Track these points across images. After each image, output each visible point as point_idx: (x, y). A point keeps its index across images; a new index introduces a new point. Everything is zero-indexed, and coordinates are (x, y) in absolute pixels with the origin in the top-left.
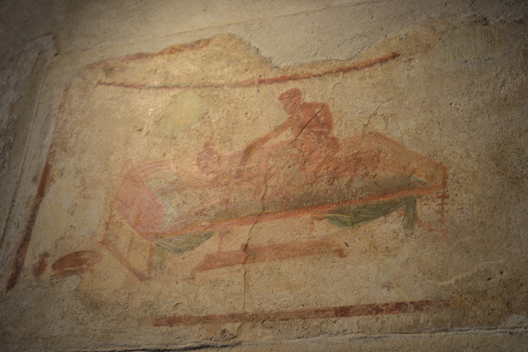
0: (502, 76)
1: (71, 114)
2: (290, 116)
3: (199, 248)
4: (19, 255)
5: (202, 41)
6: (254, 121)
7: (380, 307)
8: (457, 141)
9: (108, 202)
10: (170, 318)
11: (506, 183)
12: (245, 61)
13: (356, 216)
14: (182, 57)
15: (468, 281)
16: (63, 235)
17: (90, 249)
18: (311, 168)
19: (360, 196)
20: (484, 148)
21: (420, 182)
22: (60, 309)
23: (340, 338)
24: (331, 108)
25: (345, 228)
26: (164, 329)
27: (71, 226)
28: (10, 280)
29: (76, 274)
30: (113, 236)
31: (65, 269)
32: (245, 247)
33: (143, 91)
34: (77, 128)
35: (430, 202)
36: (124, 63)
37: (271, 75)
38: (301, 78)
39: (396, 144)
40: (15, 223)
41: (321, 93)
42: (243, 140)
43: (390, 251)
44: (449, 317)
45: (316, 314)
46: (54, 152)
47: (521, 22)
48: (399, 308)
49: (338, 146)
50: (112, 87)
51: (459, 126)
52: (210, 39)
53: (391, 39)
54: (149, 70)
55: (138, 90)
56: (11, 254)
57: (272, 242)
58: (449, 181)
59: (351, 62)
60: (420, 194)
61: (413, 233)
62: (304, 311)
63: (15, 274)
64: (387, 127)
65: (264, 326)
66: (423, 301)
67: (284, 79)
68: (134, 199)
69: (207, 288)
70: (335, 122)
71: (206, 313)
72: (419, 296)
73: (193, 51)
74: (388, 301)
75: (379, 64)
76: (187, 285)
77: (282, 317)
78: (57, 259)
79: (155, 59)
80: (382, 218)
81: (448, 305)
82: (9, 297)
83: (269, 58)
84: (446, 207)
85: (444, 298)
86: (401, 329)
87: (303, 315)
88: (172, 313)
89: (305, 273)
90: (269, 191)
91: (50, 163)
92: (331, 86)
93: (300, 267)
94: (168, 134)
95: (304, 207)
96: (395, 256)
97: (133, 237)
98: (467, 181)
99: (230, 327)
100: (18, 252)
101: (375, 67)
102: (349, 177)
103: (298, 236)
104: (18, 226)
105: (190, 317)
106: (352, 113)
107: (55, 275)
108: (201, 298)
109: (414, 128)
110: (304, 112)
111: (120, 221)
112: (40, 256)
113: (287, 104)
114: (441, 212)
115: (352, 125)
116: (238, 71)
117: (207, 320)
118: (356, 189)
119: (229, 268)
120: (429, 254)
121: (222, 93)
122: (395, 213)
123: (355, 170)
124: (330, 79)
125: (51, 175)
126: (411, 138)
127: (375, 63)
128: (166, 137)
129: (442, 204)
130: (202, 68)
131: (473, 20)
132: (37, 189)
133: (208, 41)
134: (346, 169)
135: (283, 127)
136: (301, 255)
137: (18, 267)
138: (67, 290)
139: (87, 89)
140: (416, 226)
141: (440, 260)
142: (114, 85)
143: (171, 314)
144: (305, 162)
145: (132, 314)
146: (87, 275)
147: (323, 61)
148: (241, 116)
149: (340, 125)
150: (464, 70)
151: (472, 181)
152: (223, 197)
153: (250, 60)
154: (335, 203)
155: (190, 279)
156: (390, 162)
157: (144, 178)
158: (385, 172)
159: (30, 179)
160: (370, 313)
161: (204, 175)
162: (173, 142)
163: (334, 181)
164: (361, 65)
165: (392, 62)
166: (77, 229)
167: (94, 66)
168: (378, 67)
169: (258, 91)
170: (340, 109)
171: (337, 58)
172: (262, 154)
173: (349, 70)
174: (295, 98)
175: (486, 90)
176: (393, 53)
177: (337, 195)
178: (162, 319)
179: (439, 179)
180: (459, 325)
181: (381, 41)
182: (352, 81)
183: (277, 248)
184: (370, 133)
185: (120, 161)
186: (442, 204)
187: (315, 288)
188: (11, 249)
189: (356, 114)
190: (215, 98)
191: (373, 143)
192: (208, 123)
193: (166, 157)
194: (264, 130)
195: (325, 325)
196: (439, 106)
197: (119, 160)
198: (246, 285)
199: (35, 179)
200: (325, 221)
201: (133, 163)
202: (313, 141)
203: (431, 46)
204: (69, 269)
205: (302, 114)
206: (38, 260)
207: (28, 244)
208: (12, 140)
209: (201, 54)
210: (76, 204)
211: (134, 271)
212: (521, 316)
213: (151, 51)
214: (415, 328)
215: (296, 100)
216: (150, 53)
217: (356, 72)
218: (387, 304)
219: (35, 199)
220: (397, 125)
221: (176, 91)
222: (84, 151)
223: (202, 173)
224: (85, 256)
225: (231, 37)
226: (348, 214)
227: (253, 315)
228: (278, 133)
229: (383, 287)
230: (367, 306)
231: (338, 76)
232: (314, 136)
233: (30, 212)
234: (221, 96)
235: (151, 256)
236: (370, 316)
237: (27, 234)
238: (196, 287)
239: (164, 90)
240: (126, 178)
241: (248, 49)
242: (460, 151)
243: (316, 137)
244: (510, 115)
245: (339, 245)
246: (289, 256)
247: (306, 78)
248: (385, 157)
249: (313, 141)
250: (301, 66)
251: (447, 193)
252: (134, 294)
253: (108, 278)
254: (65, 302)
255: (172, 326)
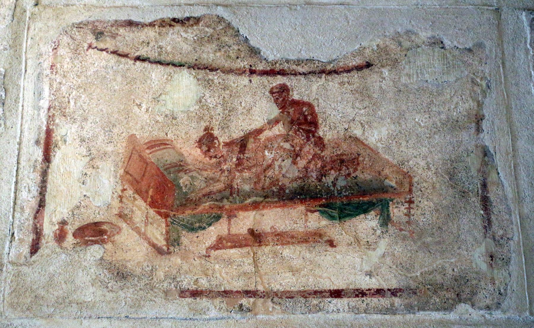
0: (455, 100)
1: (65, 76)
2: (281, 110)
3: (212, 228)
4: (36, 221)
5: (192, 19)
6: (249, 110)
7: (365, 291)
8: (420, 154)
9: (118, 176)
10: (193, 291)
11: (457, 196)
12: (236, 48)
13: (341, 211)
14: (173, 33)
15: (430, 275)
16: (79, 204)
17: (107, 221)
18: (302, 163)
19: (345, 194)
20: (441, 163)
21: (392, 187)
22: (89, 276)
23: (335, 316)
24: (316, 108)
25: (334, 221)
26: (190, 300)
27: (85, 196)
28: (33, 245)
29: (98, 244)
30: (128, 210)
31: (86, 238)
32: (251, 232)
33: (138, 63)
34: (74, 93)
35: (399, 206)
36: (114, 28)
37: (260, 67)
38: (288, 74)
39: (372, 150)
40: (25, 187)
41: (306, 92)
42: (240, 128)
43: (370, 245)
44: (416, 303)
45: (315, 294)
46: (54, 115)
47: (470, 50)
48: (379, 293)
49: (324, 146)
50: (104, 52)
51: (422, 141)
52: (199, 19)
53: (365, 48)
54: (141, 41)
55: (133, 62)
56: (27, 219)
57: (274, 229)
58: (414, 189)
59: (332, 65)
60: (392, 197)
61: (387, 231)
62: (305, 291)
63: (36, 240)
64: (364, 133)
65: (273, 303)
66: (397, 289)
67: (272, 73)
68: (144, 175)
69: (222, 266)
70: (320, 122)
71: (225, 288)
72: (394, 284)
73: (184, 28)
74: (371, 287)
75: (355, 71)
76: (203, 262)
77: (288, 295)
78: (76, 228)
79: (146, 30)
80: (362, 216)
81: (415, 293)
82: (34, 262)
83: (258, 49)
84: (412, 211)
85: (412, 288)
86: (381, 311)
87: (306, 294)
88: (194, 286)
89: (304, 258)
90: (268, 180)
91: (51, 127)
92: (314, 87)
93: (299, 253)
94: (168, 112)
95: (299, 199)
96: (374, 249)
97: (148, 212)
98: (428, 191)
99: (245, 301)
100: (35, 218)
101: (352, 73)
102: (334, 176)
103: (295, 225)
104: (29, 190)
105: (210, 291)
106: (334, 115)
107: (77, 243)
108: (218, 275)
109: (386, 138)
110: (293, 109)
111: (132, 196)
112: (59, 223)
113: (277, 99)
114: (408, 215)
115: (335, 128)
116: (229, 57)
117: (226, 293)
118: (341, 187)
119: (240, 249)
120: (400, 250)
121: (216, 78)
122: (372, 212)
123: (340, 170)
124: (314, 79)
125: (54, 140)
126: (384, 146)
127: (352, 69)
128: (166, 116)
129: (409, 208)
130: (194, 49)
131: (433, 41)
132: (42, 154)
133: (198, 20)
134: (332, 168)
135: (277, 122)
136: (299, 242)
137: (38, 233)
138: (92, 258)
139: (78, 52)
140: (390, 226)
141: (408, 255)
142: (107, 52)
143: (193, 288)
144: (297, 157)
145: (157, 286)
146: (109, 246)
147: (307, 60)
148: (236, 104)
149: (325, 126)
150: (425, 88)
151: (432, 191)
152: (227, 183)
153: (240, 47)
154: (324, 198)
155: (206, 256)
156: (368, 166)
157: (150, 156)
158: (364, 175)
159: (33, 141)
160: (357, 296)
161: (207, 159)
162: (174, 122)
163: (322, 178)
164: (341, 70)
165: (366, 71)
166: (91, 199)
167: (82, 26)
168: (355, 75)
169: (250, 81)
170: (324, 110)
171: (319, 59)
172: (259, 145)
173: (330, 73)
174: (284, 94)
175: (442, 110)
176: (367, 62)
177: (325, 192)
178: (186, 291)
179: (407, 186)
180: (424, 310)
181: (356, 48)
182: (333, 84)
183: (278, 235)
184: (350, 137)
185: (124, 134)
186: (409, 208)
187: (313, 272)
188: (27, 214)
189: (338, 117)
190: (210, 82)
191: (353, 147)
192: (205, 107)
193: (169, 136)
194: (258, 122)
195: (323, 304)
196: (405, 119)
197: (122, 133)
198: (256, 266)
199: (37, 142)
200: (317, 214)
201: (136, 138)
202: (303, 138)
203: (399, 61)
204: (90, 238)
205: (291, 111)
206: (57, 227)
207: (44, 210)
208: (4, 96)
209: (192, 33)
210: (86, 174)
211: (154, 246)
212: (467, 305)
213: (142, 21)
214: (391, 310)
215: (285, 96)
216: (140, 22)
217: (336, 76)
218: (369, 290)
219: (42, 164)
220: (372, 132)
221: (170, 69)
222: (86, 119)
223: (205, 157)
224: (104, 227)
225: (221, 19)
226: (335, 209)
227: (264, 292)
228: (271, 127)
229: (366, 275)
230: (355, 290)
231: (321, 78)
232: (303, 134)
233: (39, 177)
234: (216, 81)
235: (167, 232)
236: (357, 299)
237: (41, 200)
238: (212, 265)
239: (159, 66)
240: (132, 153)
241: (237, 35)
242: (423, 163)
243: (305, 135)
244: (460, 136)
245: (329, 237)
246: (288, 243)
247: (293, 74)
248: (363, 161)
249: (303, 138)
250: (288, 61)
251: (412, 199)
252: (157, 267)
253: (130, 250)
254: (92, 270)
255: (195, 299)
